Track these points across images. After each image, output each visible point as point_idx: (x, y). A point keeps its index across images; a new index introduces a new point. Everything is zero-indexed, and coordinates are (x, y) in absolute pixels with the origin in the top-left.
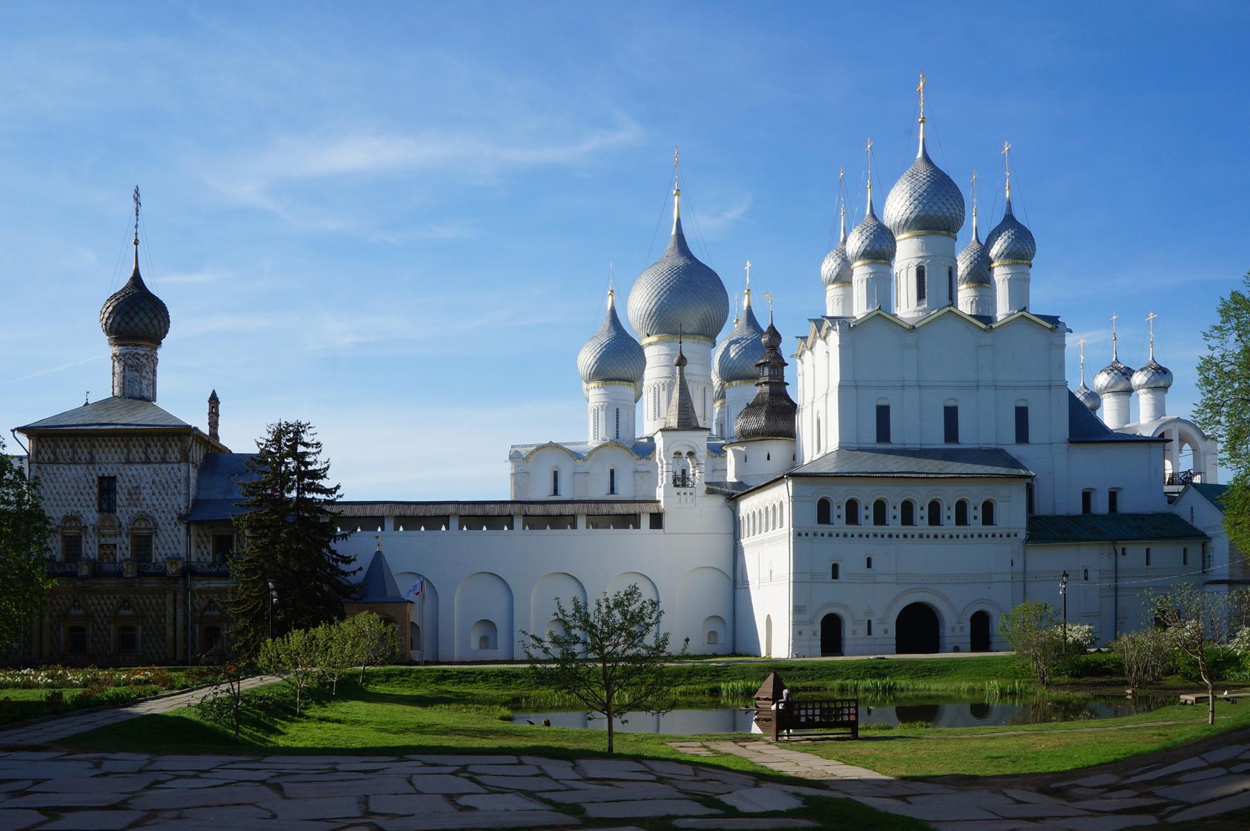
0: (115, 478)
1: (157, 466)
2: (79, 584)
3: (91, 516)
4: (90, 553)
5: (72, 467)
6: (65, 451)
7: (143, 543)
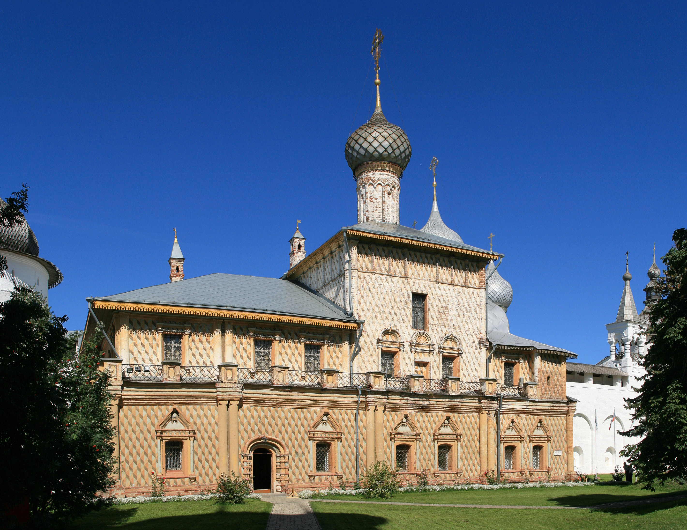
0: (427, 294)
3: (407, 333)
4: (406, 370)
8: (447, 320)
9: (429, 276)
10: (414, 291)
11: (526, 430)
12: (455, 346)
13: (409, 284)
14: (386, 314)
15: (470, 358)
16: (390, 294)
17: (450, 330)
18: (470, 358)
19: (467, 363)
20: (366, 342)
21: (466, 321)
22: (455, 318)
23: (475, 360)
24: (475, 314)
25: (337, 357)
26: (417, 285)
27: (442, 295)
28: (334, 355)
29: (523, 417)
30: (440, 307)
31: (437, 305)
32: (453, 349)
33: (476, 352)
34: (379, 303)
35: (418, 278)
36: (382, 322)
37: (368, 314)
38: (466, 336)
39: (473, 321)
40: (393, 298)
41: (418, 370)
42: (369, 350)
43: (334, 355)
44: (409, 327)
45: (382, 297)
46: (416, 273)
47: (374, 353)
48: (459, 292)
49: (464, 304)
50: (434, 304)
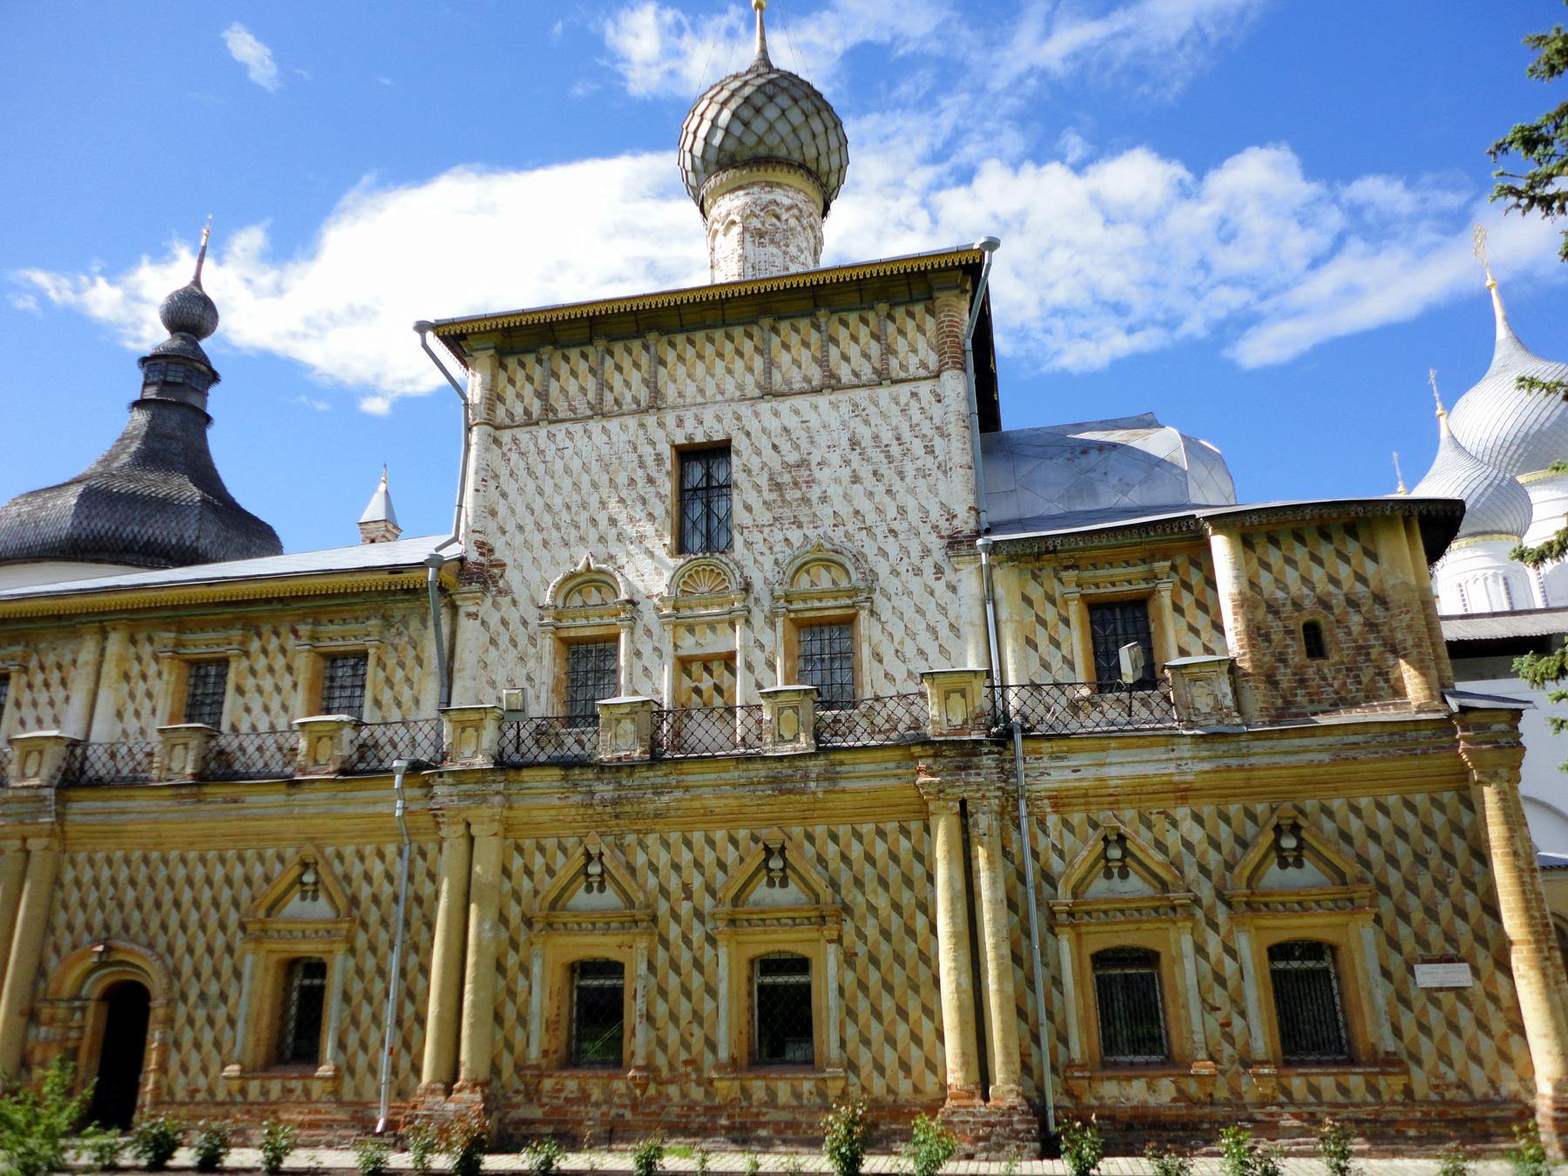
0: (729, 441)
1: (861, 395)
2: (604, 790)
3: (649, 570)
5: (595, 426)
6: (573, 380)
7: (825, 638)
8: (806, 501)
9: (740, 387)
10: (680, 440)
11: (1204, 870)
12: (844, 584)
13: (661, 425)
14: (577, 527)
15: (909, 613)
16: (595, 467)
17: (820, 531)
18: (909, 613)
19: (899, 633)
20: (504, 623)
21: (889, 492)
22: (840, 490)
23: (933, 615)
24: (929, 462)
25: (408, 680)
26: (690, 425)
27: (786, 430)
28: (399, 675)
29: (1182, 813)
30: (777, 467)
31: (764, 464)
32: (836, 593)
33: (940, 587)
34: (557, 502)
35: (700, 399)
36: (564, 554)
37: (519, 539)
38: (891, 539)
39: (921, 482)
40: (605, 477)
41: (703, 686)
42: (515, 646)
43: (399, 675)
44: (662, 553)
45: (567, 483)
46: (691, 389)
47: (532, 650)
48: (856, 406)
49: (876, 437)
50: (755, 463)
